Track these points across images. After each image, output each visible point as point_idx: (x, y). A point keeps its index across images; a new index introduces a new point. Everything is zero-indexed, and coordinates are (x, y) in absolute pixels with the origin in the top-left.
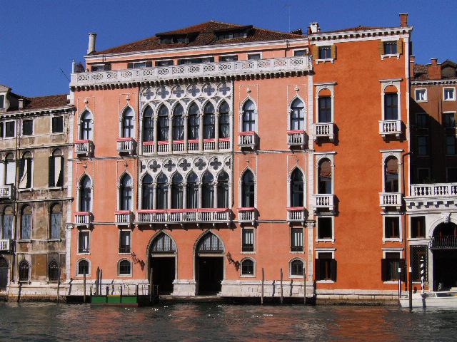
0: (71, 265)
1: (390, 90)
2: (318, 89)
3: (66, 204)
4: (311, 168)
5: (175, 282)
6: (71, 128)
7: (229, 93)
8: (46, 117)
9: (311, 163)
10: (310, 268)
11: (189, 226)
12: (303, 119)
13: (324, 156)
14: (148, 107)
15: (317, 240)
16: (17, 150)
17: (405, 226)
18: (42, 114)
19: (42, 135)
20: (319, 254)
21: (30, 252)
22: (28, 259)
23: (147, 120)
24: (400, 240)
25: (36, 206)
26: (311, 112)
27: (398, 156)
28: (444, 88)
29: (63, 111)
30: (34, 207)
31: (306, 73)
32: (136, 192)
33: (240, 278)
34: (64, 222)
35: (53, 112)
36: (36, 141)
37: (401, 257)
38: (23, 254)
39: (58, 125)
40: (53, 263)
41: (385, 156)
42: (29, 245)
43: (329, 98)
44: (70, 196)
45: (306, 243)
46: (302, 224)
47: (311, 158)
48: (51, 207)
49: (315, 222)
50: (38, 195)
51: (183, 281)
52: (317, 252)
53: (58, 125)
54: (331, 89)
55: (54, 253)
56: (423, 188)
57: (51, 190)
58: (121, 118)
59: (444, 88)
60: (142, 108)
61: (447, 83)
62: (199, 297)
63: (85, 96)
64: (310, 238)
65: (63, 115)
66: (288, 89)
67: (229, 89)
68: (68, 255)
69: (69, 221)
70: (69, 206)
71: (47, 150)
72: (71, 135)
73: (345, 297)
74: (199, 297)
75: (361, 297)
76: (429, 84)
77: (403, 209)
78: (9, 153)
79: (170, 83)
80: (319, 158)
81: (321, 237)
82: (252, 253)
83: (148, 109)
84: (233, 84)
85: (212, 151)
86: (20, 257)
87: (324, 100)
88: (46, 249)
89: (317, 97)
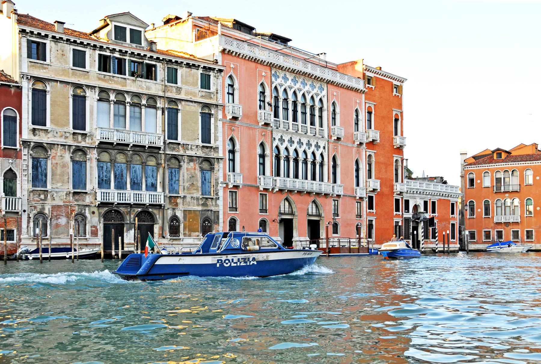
0: (224, 222)
2: (367, 105)
3: (218, 162)
8: (194, 71)
19: (190, 88)
21: (181, 207)
22: (179, 214)
25: (186, 160)
35: (204, 67)
36: (183, 92)
38: (174, 209)
39: (206, 83)
40: (207, 219)
42: (179, 201)
44: (221, 155)
50: (188, 150)
53: (206, 83)
55: (208, 210)
57: (203, 146)
70: (221, 165)
72: (220, 95)
78: (152, 98)
80: (368, 154)
86: (170, 213)
88: (198, 205)
89: (367, 111)
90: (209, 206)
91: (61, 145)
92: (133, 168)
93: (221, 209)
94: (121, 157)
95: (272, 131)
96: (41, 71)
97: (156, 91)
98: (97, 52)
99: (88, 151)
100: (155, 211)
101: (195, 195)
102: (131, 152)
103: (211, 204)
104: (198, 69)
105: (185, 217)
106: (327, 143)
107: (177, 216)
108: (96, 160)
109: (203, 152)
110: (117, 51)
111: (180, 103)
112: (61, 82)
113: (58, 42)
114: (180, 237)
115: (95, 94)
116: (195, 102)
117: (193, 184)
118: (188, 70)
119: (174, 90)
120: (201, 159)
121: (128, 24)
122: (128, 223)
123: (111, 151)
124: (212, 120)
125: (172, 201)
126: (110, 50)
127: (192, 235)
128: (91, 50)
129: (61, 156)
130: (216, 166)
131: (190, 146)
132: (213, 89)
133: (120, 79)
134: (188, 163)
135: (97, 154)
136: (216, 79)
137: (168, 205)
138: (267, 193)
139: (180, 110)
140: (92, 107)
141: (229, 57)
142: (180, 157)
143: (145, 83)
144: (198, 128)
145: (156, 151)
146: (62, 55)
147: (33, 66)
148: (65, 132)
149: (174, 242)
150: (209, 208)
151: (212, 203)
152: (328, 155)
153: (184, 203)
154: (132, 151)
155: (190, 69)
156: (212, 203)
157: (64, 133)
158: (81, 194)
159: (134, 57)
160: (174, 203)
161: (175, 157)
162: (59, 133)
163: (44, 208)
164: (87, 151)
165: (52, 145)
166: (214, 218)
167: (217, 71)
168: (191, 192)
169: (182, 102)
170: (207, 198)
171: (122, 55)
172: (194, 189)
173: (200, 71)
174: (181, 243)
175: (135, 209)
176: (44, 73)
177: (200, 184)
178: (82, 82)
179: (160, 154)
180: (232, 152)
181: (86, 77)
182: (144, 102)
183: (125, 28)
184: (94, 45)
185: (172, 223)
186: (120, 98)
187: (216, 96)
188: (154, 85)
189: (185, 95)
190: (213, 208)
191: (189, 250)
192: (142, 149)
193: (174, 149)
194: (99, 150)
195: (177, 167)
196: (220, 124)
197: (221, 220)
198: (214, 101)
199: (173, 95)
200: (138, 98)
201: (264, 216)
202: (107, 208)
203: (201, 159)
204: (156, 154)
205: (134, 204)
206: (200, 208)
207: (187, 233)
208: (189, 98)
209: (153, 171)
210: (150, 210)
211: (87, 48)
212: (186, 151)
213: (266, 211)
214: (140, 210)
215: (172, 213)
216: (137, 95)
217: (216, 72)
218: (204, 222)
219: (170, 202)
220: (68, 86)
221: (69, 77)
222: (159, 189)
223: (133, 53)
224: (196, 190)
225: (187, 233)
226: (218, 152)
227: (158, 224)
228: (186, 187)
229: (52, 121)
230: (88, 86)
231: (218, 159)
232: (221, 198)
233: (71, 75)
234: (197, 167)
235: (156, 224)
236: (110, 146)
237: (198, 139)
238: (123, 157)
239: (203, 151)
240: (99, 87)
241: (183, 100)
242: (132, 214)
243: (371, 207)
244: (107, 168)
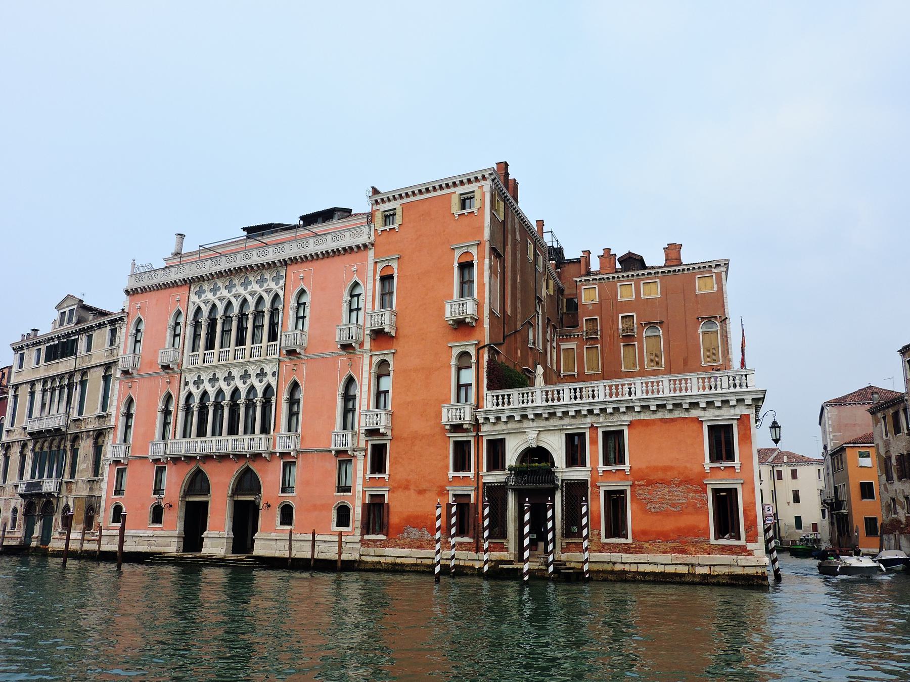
1: (466, 259)
2: (380, 266)
4: (366, 375)
5: (205, 534)
6: (123, 340)
7: (282, 282)
9: (366, 368)
10: (357, 513)
11: (223, 457)
12: (360, 309)
13: (382, 357)
14: (199, 310)
15: (369, 475)
16: (76, 371)
17: (480, 455)
18: (100, 326)
20: (371, 496)
21: (74, 493)
23: (197, 325)
24: (471, 474)
26: (370, 299)
27: (472, 351)
28: (619, 284)
30: (82, 439)
31: (365, 246)
33: (275, 531)
37: (472, 501)
41: (455, 352)
43: (391, 277)
44: (113, 423)
45: (355, 482)
46: (349, 452)
47: (366, 361)
48: (97, 438)
49: (366, 450)
51: (214, 533)
52: (367, 494)
54: (395, 265)
55: (92, 496)
56: (503, 396)
58: (171, 322)
59: (619, 284)
61: (623, 277)
62: (234, 556)
63: (140, 300)
64: (360, 474)
66: (344, 269)
68: (104, 498)
70: (111, 436)
71: (99, 368)
72: (121, 349)
73: (399, 561)
74: (234, 556)
75: (419, 561)
76: (600, 279)
77: (477, 426)
79: (220, 275)
80: (376, 360)
81: (373, 471)
82: (291, 494)
83: (199, 310)
87: (386, 279)
89: (378, 277)
93: (104, 494)
95: (181, 374)
116: (100, 366)
121: (67, 307)
125: (68, 488)
133: (55, 365)
141: (137, 296)
142: (80, 435)
144: (98, 398)
180: (128, 416)
193: (78, 427)
197: (102, 509)
216: (61, 377)
217: (120, 322)
226: (110, 420)
232: (106, 480)
243: (378, 464)
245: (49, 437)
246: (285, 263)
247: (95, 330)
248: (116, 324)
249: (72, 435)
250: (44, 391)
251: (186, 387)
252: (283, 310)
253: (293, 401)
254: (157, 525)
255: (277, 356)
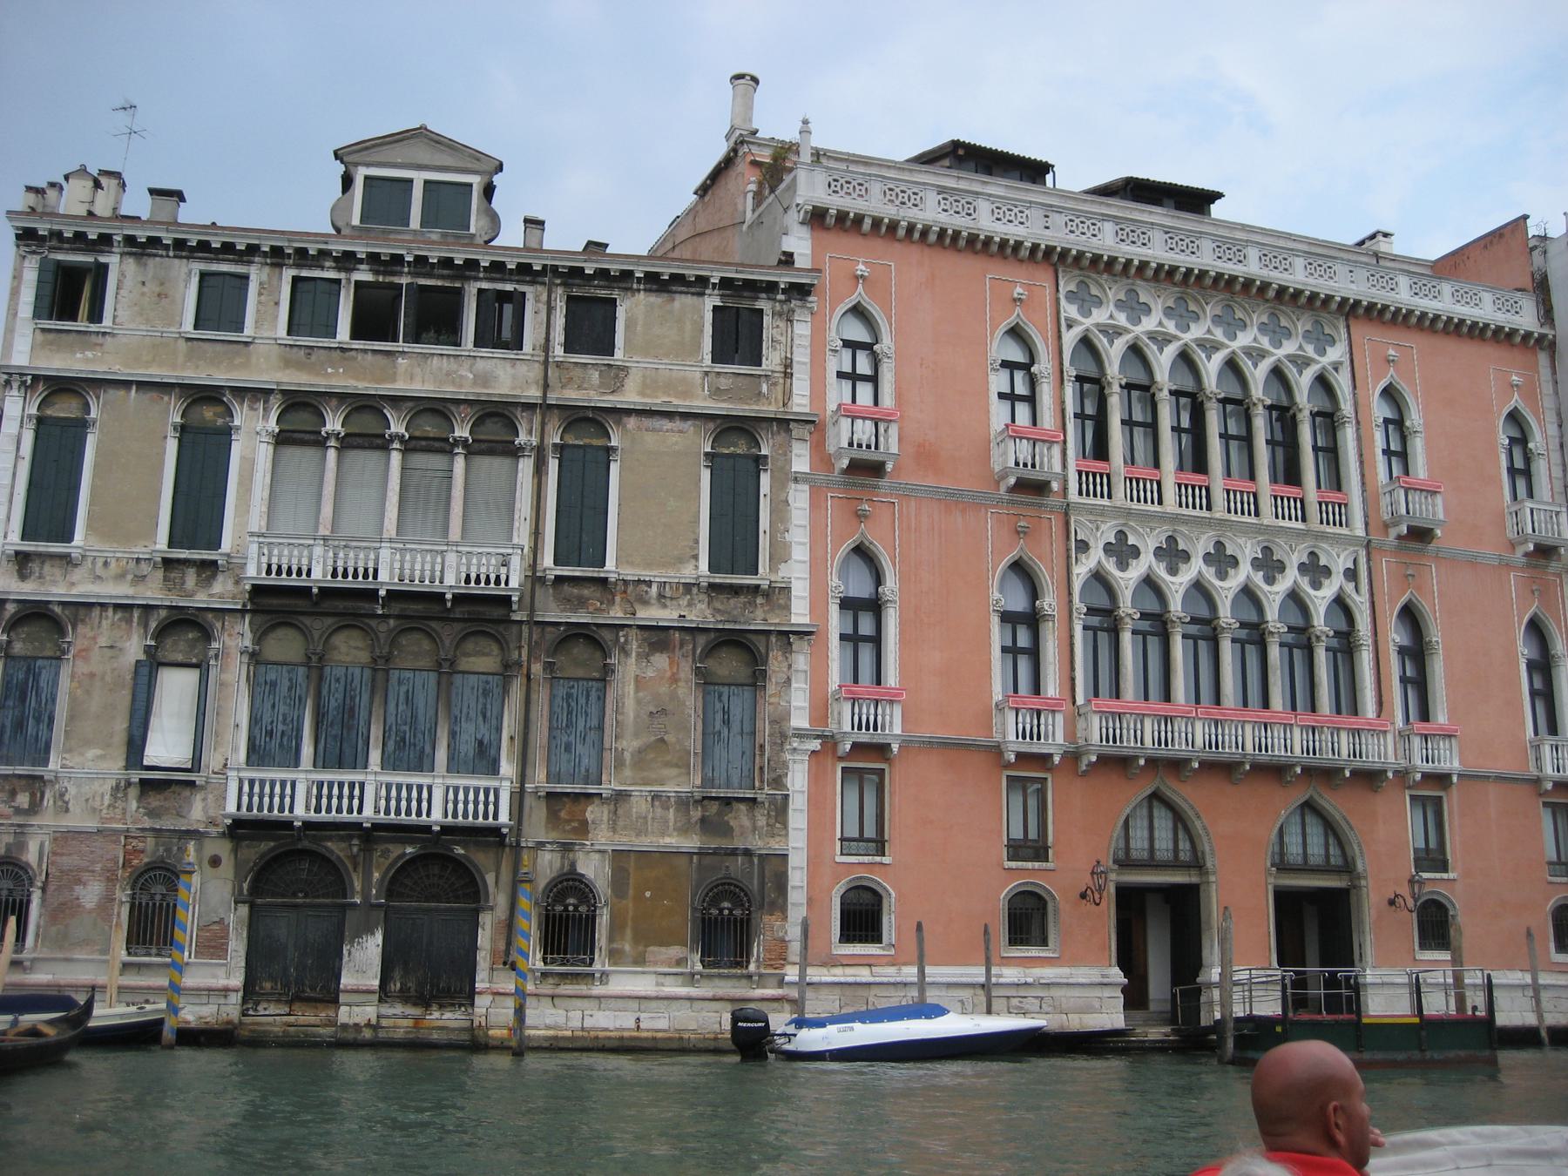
0: (810, 902)
3: (787, 648)
7: (1336, 353)
8: (683, 302)
19: (667, 367)
21: (602, 838)
22: (592, 868)
29: (771, 287)
30: (625, 651)
32: (1065, 635)
34: (781, 719)
35: (726, 283)
38: (566, 848)
40: (729, 890)
42: (593, 812)
44: (800, 615)
50: (645, 602)
55: (733, 852)
60: (1070, 338)
65: (763, 304)
67: (1333, 342)
68: (798, 863)
69: (799, 721)
70: (801, 661)
79: (1165, 275)
83: (1086, 342)
84: (1348, 327)
85: (1300, 525)
86: (547, 865)
88: (684, 830)
90: (737, 831)
91: (117, 607)
92: (400, 682)
94: (352, 643)
95: (1066, 514)
96: (78, 355)
97: (514, 388)
98: (288, 274)
99: (219, 625)
100: (481, 859)
101: (670, 788)
102: (392, 622)
103: (746, 822)
104: (702, 294)
105: (619, 881)
106: (1362, 553)
107: (580, 878)
108: (246, 659)
109: (718, 611)
110: (361, 261)
111: (618, 423)
112: (143, 385)
113: (150, 255)
114: (597, 966)
115: (266, 417)
116: (686, 416)
117: (662, 740)
118: (654, 299)
119: (595, 376)
120: (702, 640)
122: (355, 904)
123: (307, 621)
124: (765, 480)
125: (563, 814)
126: (336, 259)
127: (649, 957)
128: (267, 269)
129: (112, 647)
130: (775, 663)
131: (654, 589)
132: (771, 360)
133: (369, 356)
134: (645, 656)
135: (249, 635)
136: (782, 324)
137: (543, 831)
138: (1048, 776)
139: (614, 449)
140: (249, 464)
142: (607, 635)
143: (469, 362)
145: (497, 613)
146: (159, 295)
147: (51, 343)
148: (138, 560)
149: (568, 989)
150: (739, 844)
151: (753, 819)
152: (1373, 604)
153: (621, 823)
154: (398, 617)
155: (666, 295)
156: (753, 819)
157: (132, 564)
158: (173, 788)
159: (429, 276)
160: (568, 821)
161: (585, 635)
162: (113, 564)
163: (22, 846)
164: (212, 627)
165: (82, 608)
166: (762, 884)
167: (784, 291)
168: (653, 776)
169: (625, 419)
170: (727, 802)
171: (385, 273)
172: (667, 764)
173: (711, 301)
174: (598, 990)
175: (391, 847)
176: (87, 360)
177: (694, 742)
178: (219, 376)
179: (515, 629)
181: (237, 361)
182: (462, 432)
183: (411, 181)
184: (272, 247)
185: (559, 908)
186: (367, 423)
187: (780, 388)
188: (508, 365)
189: (642, 394)
190: (757, 844)
191: (631, 1024)
192: (435, 608)
193: (582, 603)
194: (260, 619)
195: (596, 675)
196: (799, 498)
198: (772, 408)
199: (587, 392)
200: (438, 420)
201: (1029, 873)
202: (272, 844)
203: (702, 640)
204: (501, 628)
205: (377, 827)
206: (691, 843)
207: (627, 947)
208: (659, 401)
209: (486, 693)
210: (459, 851)
211: (250, 263)
212: (638, 607)
213: (1038, 850)
214: (409, 850)
215: (557, 864)
217: (780, 297)
218: (715, 901)
219: (553, 818)
220: (166, 398)
221: (174, 367)
222: (507, 768)
223: (421, 260)
224: (677, 766)
225: (627, 947)
226: (787, 608)
227: (492, 909)
228: (627, 756)
229: (90, 526)
230: (240, 392)
231: (785, 634)
233: (181, 359)
234: (686, 670)
235: (484, 909)
236: (301, 604)
237: (696, 557)
238: (360, 644)
239: (718, 605)
240: (283, 392)
241: (629, 412)
242: (378, 867)
244: (290, 689)
245: (382, 616)
246: (1350, 310)
247: (630, 289)
248: (757, 298)
249: (549, 629)
250: (283, 440)
251: (1083, 557)
252: (1358, 423)
253: (1417, 653)
254: (1034, 952)
255: (1360, 531)
